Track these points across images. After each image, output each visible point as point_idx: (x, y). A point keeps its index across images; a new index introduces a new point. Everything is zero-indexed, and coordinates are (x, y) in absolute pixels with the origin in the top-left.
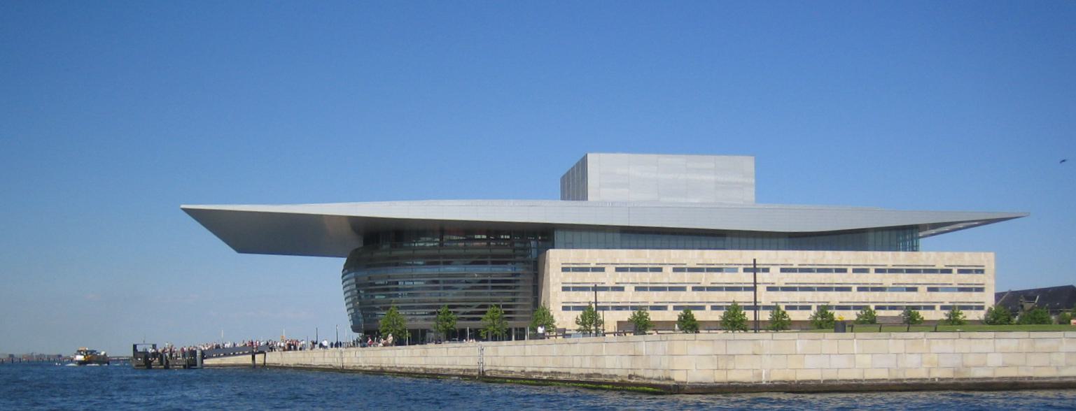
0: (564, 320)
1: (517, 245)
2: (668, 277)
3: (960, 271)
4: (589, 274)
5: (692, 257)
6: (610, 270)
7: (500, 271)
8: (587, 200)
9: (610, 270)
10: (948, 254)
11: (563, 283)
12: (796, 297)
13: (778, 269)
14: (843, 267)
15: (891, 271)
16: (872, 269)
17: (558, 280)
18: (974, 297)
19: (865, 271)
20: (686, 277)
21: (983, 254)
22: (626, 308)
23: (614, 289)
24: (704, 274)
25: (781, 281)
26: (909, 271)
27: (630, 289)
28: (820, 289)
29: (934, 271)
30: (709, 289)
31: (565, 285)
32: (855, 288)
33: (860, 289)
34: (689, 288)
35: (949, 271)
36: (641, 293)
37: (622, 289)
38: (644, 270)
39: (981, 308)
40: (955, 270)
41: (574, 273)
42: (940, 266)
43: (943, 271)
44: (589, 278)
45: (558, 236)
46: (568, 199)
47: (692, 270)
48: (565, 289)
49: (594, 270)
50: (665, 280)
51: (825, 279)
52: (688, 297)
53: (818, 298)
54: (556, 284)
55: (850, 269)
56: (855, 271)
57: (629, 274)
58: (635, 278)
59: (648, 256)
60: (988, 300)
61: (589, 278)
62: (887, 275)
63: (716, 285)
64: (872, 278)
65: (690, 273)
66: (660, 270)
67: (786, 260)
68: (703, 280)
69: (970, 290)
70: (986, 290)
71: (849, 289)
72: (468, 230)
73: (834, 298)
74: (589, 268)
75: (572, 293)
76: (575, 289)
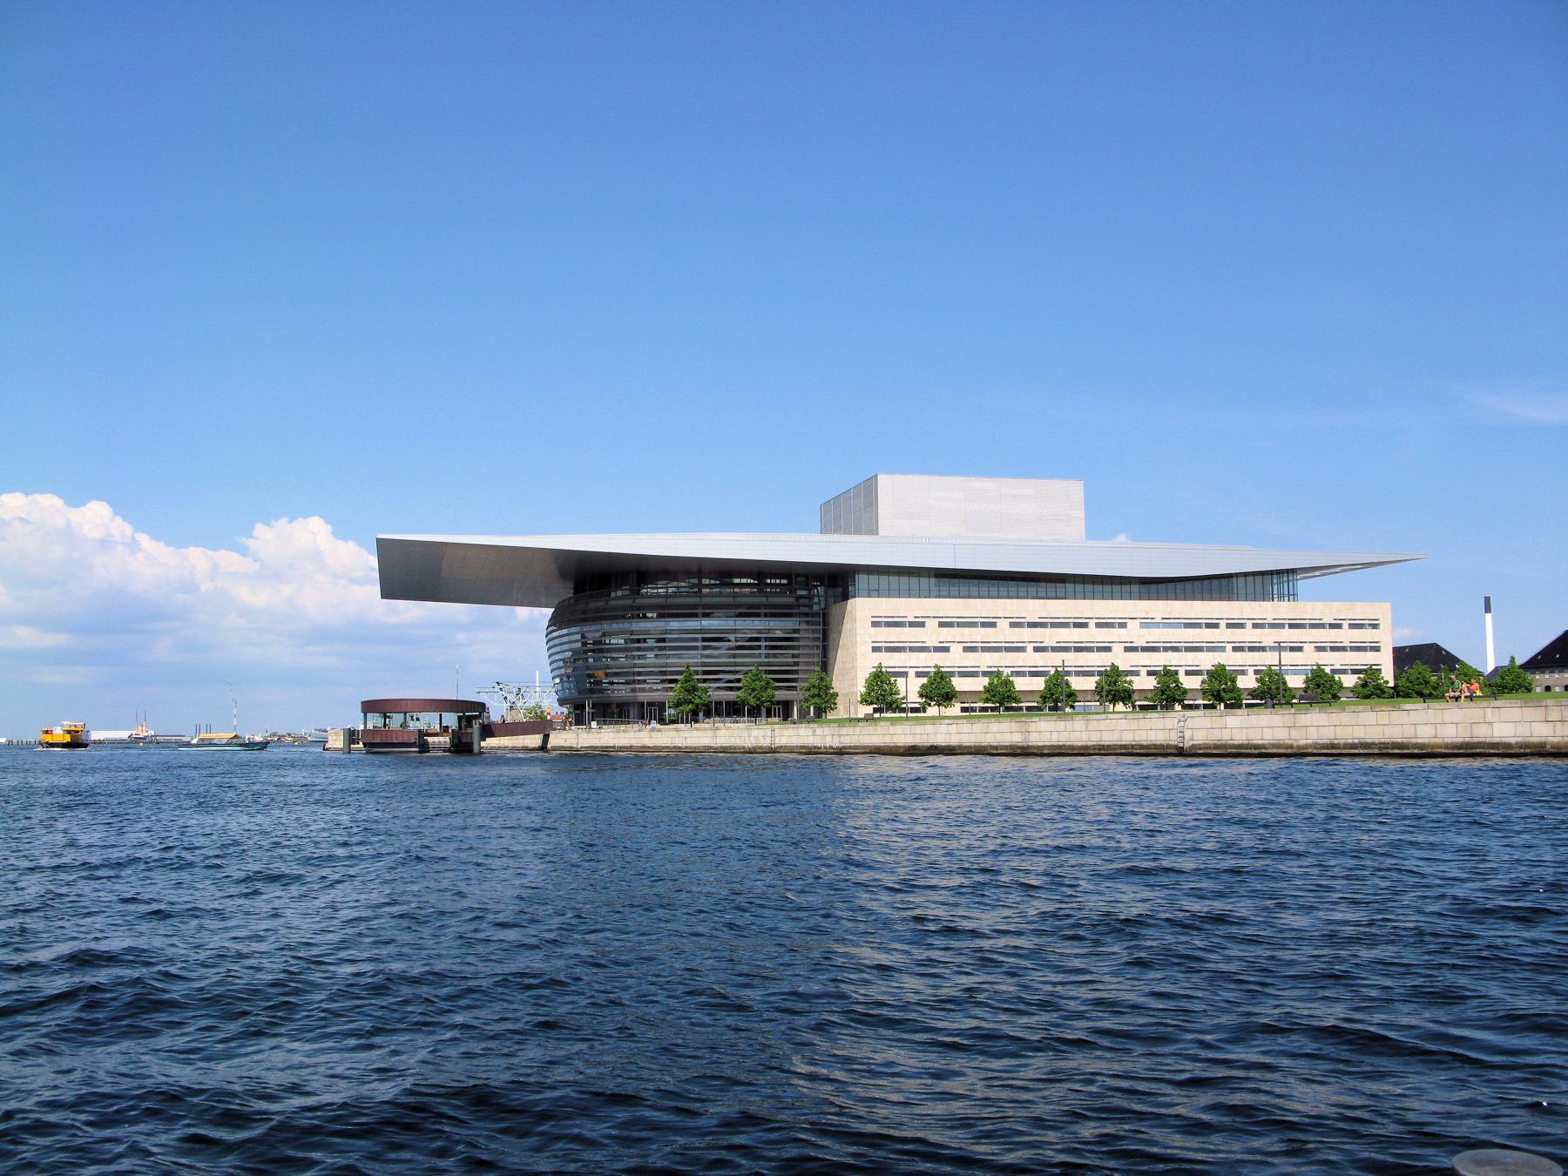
1: (800, 592)
2: (1003, 634)
3: (1352, 626)
4: (907, 630)
6: (932, 624)
7: (779, 627)
8: (877, 534)
9: (932, 624)
10: (1336, 605)
16: (1249, 624)
19: (1241, 626)
20: (1026, 634)
21: (1376, 604)
23: (938, 649)
24: (1047, 630)
26: (1292, 626)
27: (956, 649)
29: (1322, 626)
31: (875, 645)
32: (1229, 647)
33: (1235, 649)
34: (1030, 647)
35: (1338, 626)
36: (971, 655)
37: (946, 650)
38: (973, 625)
40: (1345, 624)
42: (1328, 620)
43: (1332, 626)
45: (862, 580)
46: (836, 531)
52: (1030, 659)
55: (1223, 624)
56: (1229, 626)
62: (1267, 631)
63: (1063, 645)
64: (1248, 635)
66: (993, 625)
67: (1147, 613)
69: (1363, 649)
70: (1382, 649)
72: (724, 571)
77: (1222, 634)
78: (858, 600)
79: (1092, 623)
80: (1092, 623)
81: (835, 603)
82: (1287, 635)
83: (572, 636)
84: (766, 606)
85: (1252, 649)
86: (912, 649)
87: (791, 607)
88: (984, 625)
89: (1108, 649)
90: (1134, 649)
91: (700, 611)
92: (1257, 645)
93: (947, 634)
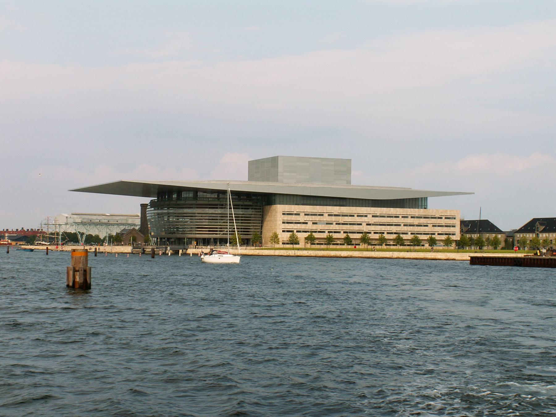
0: (283, 236)
3: (446, 218)
4: (294, 216)
5: (336, 210)
6: (302, 214)
9: (302, 214)
11: (283, 220)
13: (371, 215)
14: (398, 215)
15: (417, 217)
16: (410, 216)
17: (281, 219)
18: (451, 230)
19: (407, 217)
20: (333, 218)
23: (303, 223)
24: (340, 217)
25: (372, 221)
26: (425, 218)
27: (310, 223)
28: (388, 225)
29: (435, 218)
30: (343, 224)
32: (402, 224)
33: (404, 225)
34: (334, 223)
35: (441, 218)
37: (307, 223)
40: (444, 218)
41: (287, 216)
42: (437, 216)
43: (439, 218)
44: (293, 218)
45: (278, 199)
48: (283, 223)
49: (296, 214)
51: (390, 221)
52: (334, 227)
53: (387, 229)
54: (280, 220)
55: (400, 216)
56: (402, 217)
57: (310, 216)
58: (312, 218)
59: (318, 209)
60: (457, 230)
61: (293, 218)
62: (416, 219)
63: (346, 222)
64: (409, 221)
65: (335, 217)
66: (322, 215)
67: (374, 212)
68: (340, 220)
69: (450, 226)
70: (456, 227)
71: (399, 225)
74: (293, 214)
76: (288, 223)
77: (400, 220)
78: (278, 206)
79: (356, 215)
80: (356, 215)
81: (265, 205)
82: (423, 221)
84: (242, 206)
85: (410, 225)
86: (296, 223)
87: (250, 206)
88: (320, 215)
89: (361, 224)
90: (370, 225)
91: (219, 206)
92: (412, 224)
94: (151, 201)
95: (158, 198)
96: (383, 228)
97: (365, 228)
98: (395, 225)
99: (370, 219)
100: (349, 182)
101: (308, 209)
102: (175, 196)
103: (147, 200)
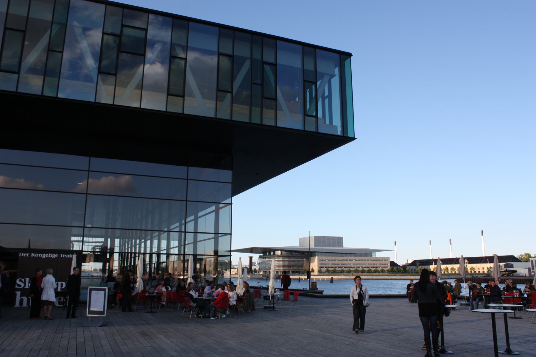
2: (337, 262)
5: (341, 258)
12: (360, 265)
15: (373, 261)
20: (340, 262)
22: (333, 268)
23: (328, 264)
26: (376, 261)
28: (362, 264)
39: (387, 268)
44: (324, 262)
45: (317, 253)
47: (341, 260)
48: (320, 264)
50: (336, 262)
52: (340, 265)
56: (367, 261)
64: (370, 262)
73: (364, 266)
75: (321, 265)
76: (322, 264)
82: (375, 262)
83: (261, 260)
84: (301, 257)
88: (334, 260)
93: (329, 262)
94: (260, 255)
95: (263, 254)
96: (360, 265)
97: (352, 266)
98: (365, 264)
99: (354, 262)
100: (343, 246)
101: (330, 258)
102: (272, 253)
103: (258, 255)
